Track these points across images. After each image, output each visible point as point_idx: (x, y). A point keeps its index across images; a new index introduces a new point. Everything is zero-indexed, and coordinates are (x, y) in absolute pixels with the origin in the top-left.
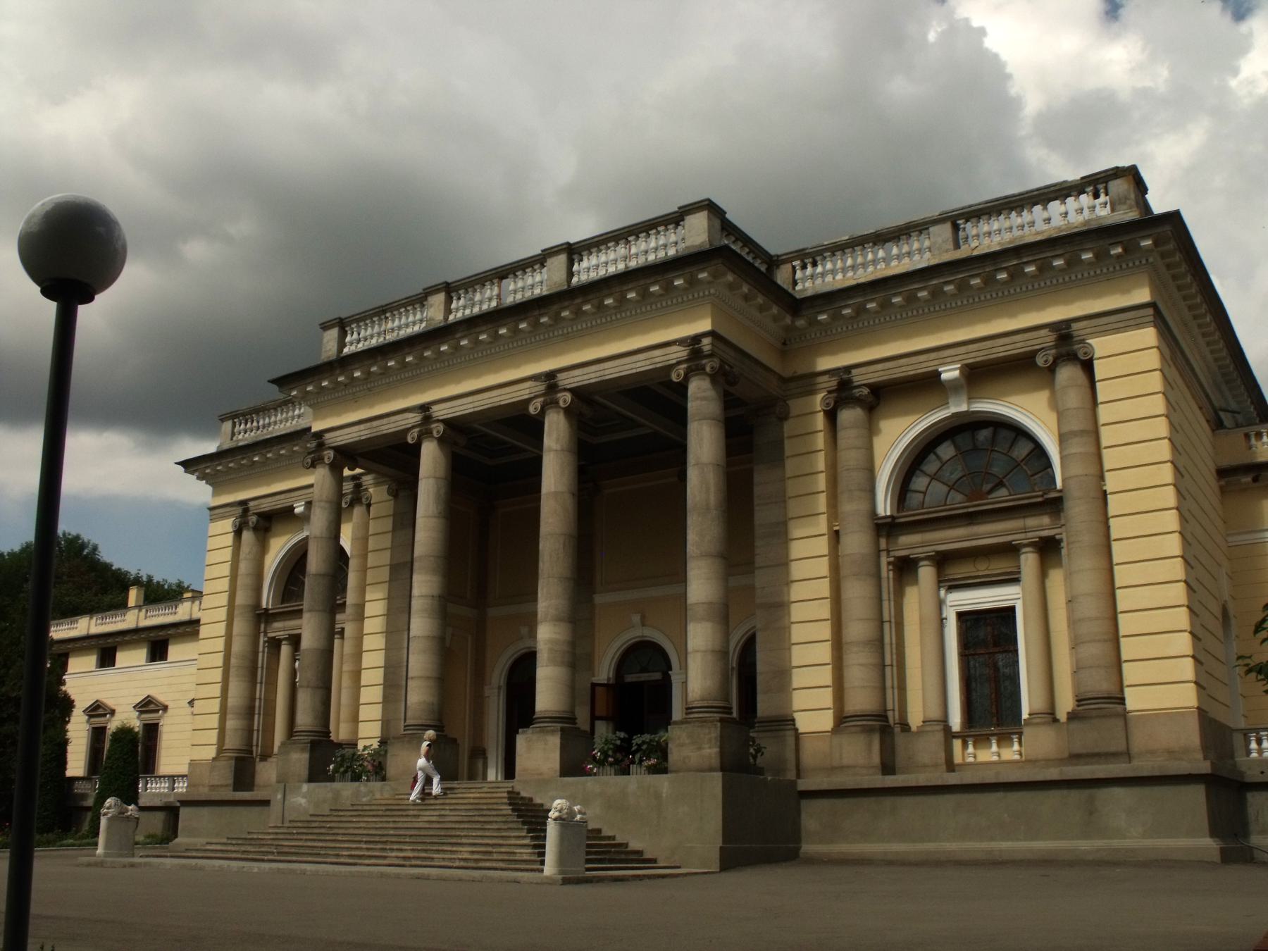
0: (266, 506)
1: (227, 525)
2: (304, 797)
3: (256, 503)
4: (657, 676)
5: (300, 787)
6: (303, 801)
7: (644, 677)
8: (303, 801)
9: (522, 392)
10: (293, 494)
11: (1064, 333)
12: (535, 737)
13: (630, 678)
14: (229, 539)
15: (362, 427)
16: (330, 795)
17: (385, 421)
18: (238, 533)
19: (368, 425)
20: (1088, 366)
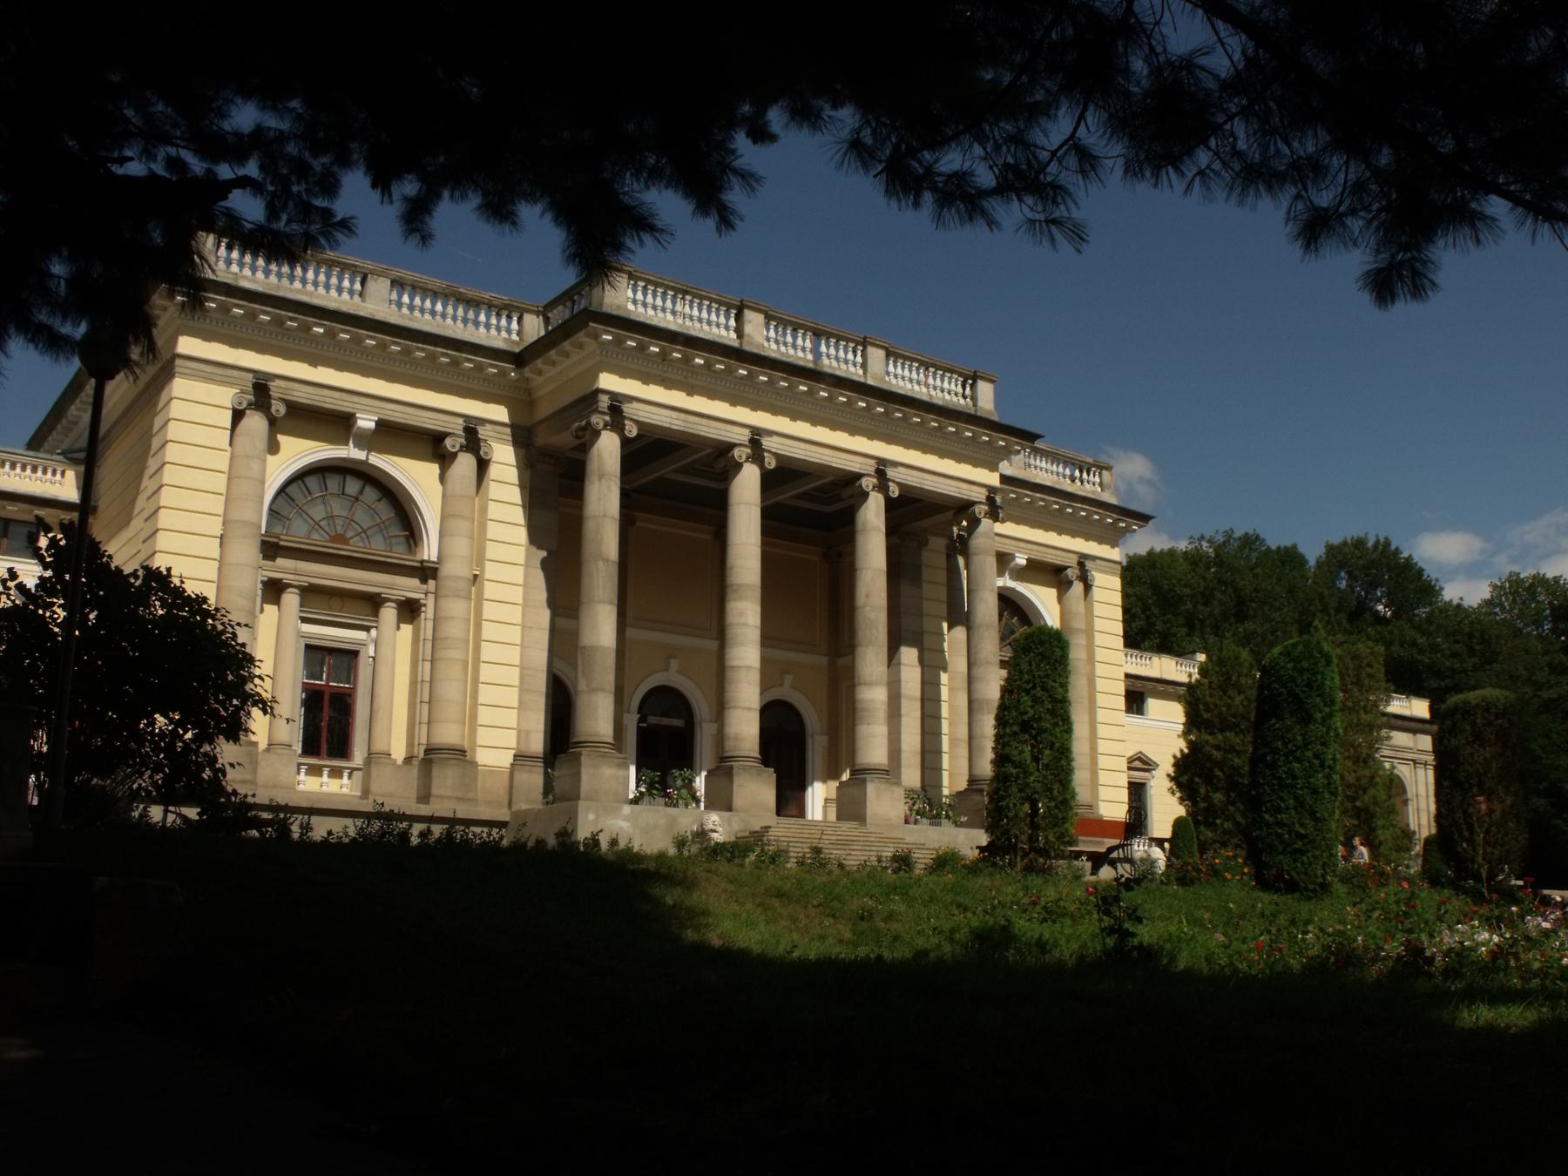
0: (303, 395)
1: (226, 396)
2: (627, 819)
3: (282, 383)
4: (678, 723)
5: (620, 809)
6: (625, 825)
7: (665, 721)
8: (625, 825)
9: (854, 464)
10: (356, 399)
11: (1083, 559)
12: (883, 787)
13: (652, 720)
14: (226, 418)
15: (675, 414)
16: (663, 821)
17: (704, 421)
18: (238, 416)
19: (683, 416)
20: (1088, 587)
